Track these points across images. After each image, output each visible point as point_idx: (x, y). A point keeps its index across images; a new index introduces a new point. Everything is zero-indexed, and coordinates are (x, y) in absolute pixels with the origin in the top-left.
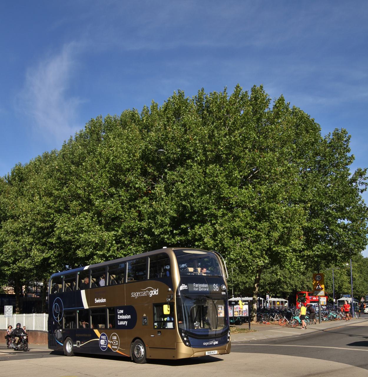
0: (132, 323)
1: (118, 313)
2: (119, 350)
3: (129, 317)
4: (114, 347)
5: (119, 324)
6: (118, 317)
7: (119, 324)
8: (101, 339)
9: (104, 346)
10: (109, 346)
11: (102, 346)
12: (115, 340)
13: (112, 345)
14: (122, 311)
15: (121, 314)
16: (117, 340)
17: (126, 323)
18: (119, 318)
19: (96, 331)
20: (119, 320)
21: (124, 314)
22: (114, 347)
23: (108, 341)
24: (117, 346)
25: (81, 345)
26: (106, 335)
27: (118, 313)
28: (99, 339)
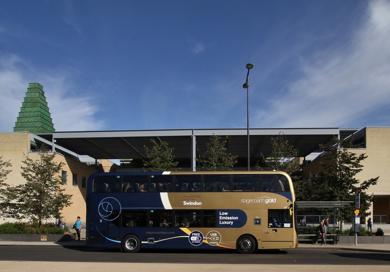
0: (238, 224)
1: (220, 214)
2: (220, 244)
3: (237, 218)
4: (212, 243)
5: (220, 223)
6: (220, 218)
7: (220, 223)
8: (191, 236)
9: (196, 242)
10: (206, 242)
11: (193, 242)
12: (214, 236)
13: (209, 240)
14: (226, 214)
15: (225, 216)
16: (218, 235)
17: (232, 223)
18: (220, 219)
19: (185, 230)
20: (221, 220)
21: (228, 216)
22: (212, 243)
23: (204, 237)
24: (218, 241)
25: (155, 242)
26: (199, 233)
27: (220, 214)
28: (189, 237)
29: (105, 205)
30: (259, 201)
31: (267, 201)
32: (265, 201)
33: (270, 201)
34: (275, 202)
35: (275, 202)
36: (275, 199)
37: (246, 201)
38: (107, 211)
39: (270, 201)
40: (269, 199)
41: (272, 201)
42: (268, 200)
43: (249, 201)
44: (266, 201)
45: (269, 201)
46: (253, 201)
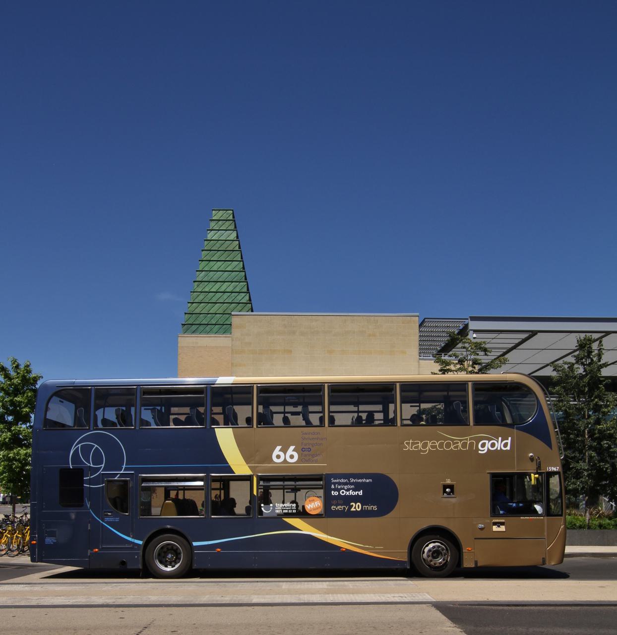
29: (86, 450)
30: (460, 444)
31: (483, 445)
32: (477, 445)
33: (493, 445)
34: (508, 448)
35: (508, 448)
36: (509, 441)
37: (420, 445)
38: (103, 465)
39: (493, 445)
40: (489, 439)
41: (499, 445)
42: (487, 442)
43: (430, 444)
44: (480, 448)
45: (488, 445)
46: (441, 445)
